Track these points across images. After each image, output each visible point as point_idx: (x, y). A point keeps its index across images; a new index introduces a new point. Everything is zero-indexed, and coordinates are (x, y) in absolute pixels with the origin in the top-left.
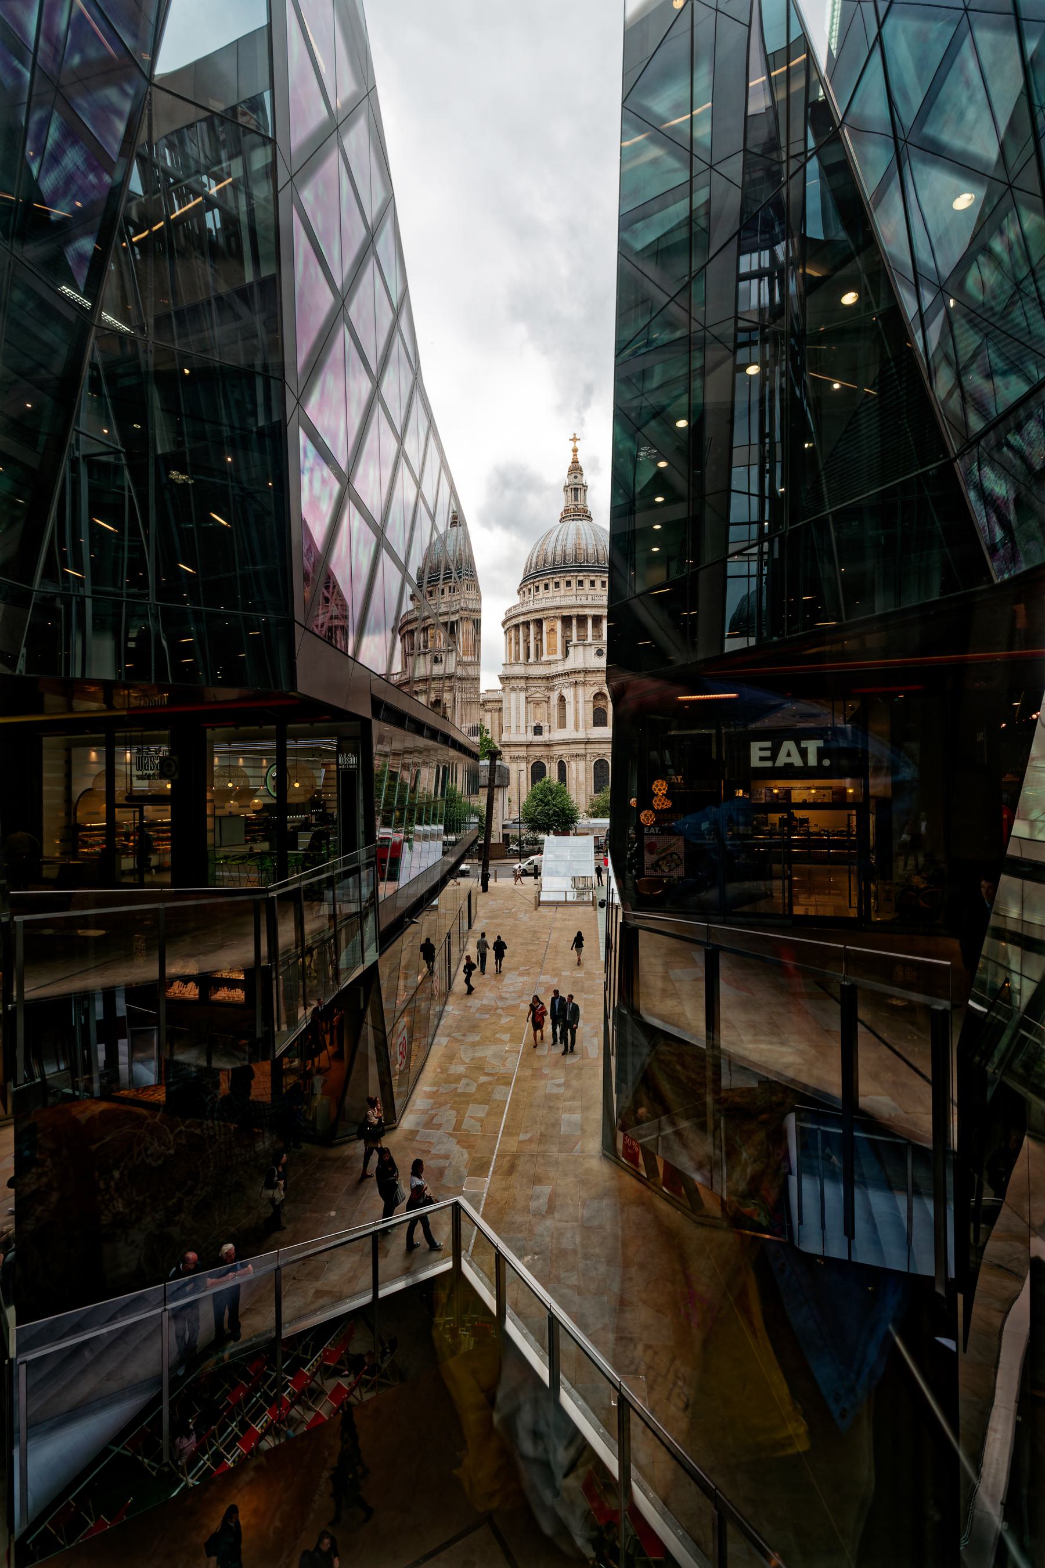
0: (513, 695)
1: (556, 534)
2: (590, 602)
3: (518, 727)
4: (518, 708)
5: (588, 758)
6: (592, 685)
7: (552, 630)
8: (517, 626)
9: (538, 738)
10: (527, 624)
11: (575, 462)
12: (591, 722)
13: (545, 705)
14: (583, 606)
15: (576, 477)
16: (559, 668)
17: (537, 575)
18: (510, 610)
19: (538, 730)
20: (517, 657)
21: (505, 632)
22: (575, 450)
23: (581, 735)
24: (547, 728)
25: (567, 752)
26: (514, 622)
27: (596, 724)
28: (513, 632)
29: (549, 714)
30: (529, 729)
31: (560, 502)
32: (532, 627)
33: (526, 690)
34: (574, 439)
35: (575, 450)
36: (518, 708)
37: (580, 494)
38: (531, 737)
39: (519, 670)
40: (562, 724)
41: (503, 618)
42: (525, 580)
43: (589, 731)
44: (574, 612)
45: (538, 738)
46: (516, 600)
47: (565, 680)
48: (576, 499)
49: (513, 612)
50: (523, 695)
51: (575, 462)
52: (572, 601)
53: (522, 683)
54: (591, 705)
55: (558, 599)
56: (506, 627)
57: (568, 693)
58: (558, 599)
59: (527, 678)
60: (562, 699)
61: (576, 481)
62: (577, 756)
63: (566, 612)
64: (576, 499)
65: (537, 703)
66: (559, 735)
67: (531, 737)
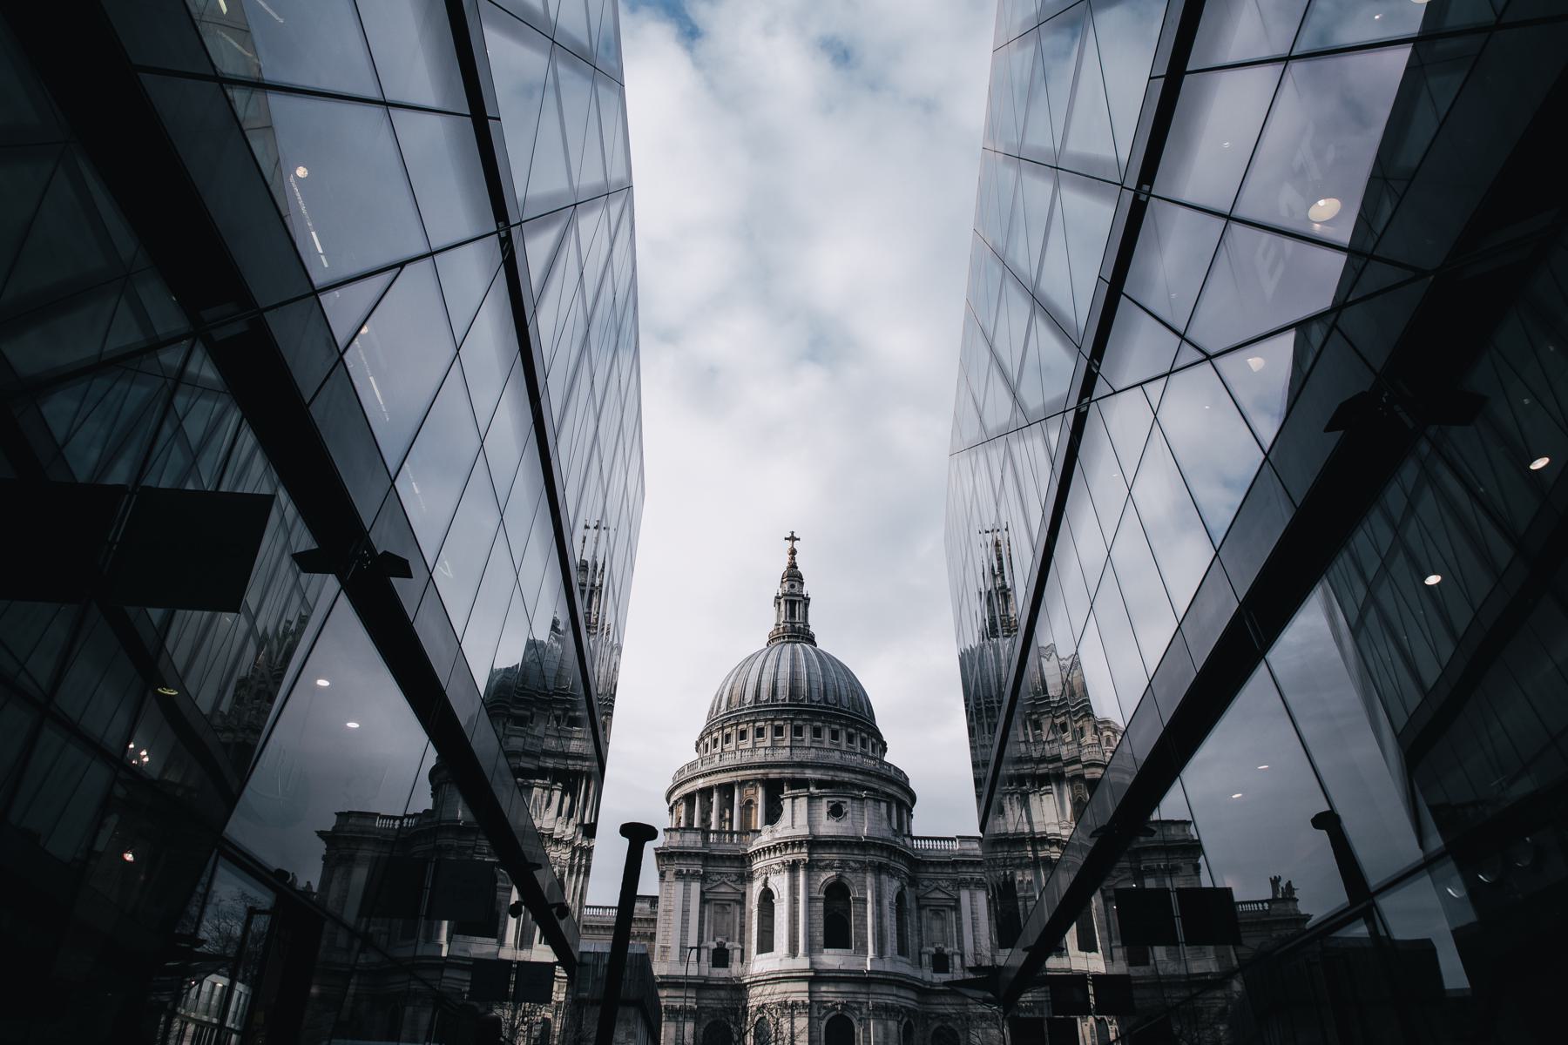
0: (678, 887)
1: (761, 658)
2: (811, 755)
3: (683, 947)
4: (685, 912)
5: (815, 1010)
6: (824, 868)
7: (748, 805)
8: (689, 798)
9: (721, 972)
10: (706, 793)
11: (793, 566)
12: (820, 938)
13: (738, 908)
14: (802, 765)
15: (792, 586)
16: (766, 838)
17: (728, 721)
18: (681, 771)
19: (721, 957)
20: (690, 817)
21: (671, 809)
22: (793, 552)
23: (802, 963)
24: (737, 954)
25: (777, 998)
26: (688, 788)
27: (827, 946)
28: (683, 808)
29: (742, 926)
30: (704, 953)
31: (769, 619)
32: (715, 798)
33: (704, 878)
34: (793, 538)
35: (793, 552)
36: (685, 912)
37: (799, 610)
38: (706, 969)
39: (692, 840)
40: (766, 945)
41: (669, 784)
42: (708, 732)
43: (817, 958)
44: (787, 773)
45: (721, 972)
46: (695, 756)
47: (775, 859)
48: (792, 615)
49: (687, 774)
50: (696, 887)
51: (793, 566)
52: (783, 755)
53: (697, 867)
54: (820, 905)
55: (762, 752)
56: (673, 799)
57: (780, 884)
58: (762, 752)
59: (707, 858)
60: (767, 896)
61: (796, 590)
62: (795, 1005)
63: (774, 774)
64: (792, 615)
65: (723, 906)
66: (761, 964)
67: (706, 969)
